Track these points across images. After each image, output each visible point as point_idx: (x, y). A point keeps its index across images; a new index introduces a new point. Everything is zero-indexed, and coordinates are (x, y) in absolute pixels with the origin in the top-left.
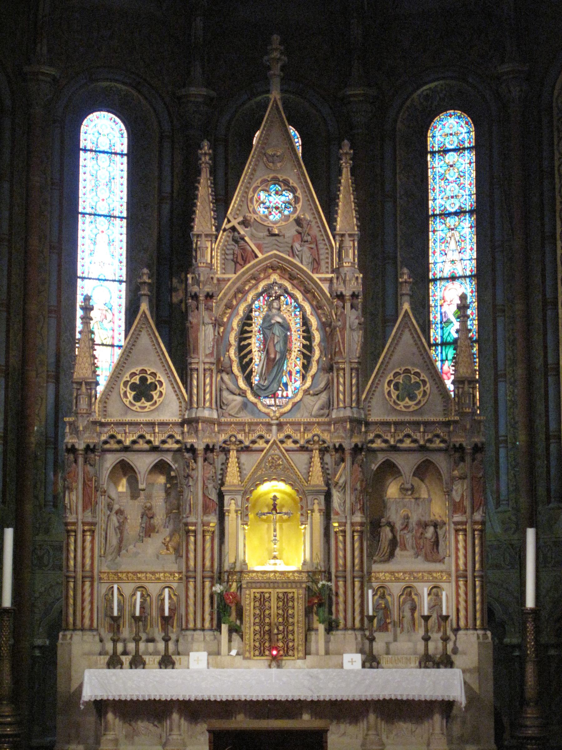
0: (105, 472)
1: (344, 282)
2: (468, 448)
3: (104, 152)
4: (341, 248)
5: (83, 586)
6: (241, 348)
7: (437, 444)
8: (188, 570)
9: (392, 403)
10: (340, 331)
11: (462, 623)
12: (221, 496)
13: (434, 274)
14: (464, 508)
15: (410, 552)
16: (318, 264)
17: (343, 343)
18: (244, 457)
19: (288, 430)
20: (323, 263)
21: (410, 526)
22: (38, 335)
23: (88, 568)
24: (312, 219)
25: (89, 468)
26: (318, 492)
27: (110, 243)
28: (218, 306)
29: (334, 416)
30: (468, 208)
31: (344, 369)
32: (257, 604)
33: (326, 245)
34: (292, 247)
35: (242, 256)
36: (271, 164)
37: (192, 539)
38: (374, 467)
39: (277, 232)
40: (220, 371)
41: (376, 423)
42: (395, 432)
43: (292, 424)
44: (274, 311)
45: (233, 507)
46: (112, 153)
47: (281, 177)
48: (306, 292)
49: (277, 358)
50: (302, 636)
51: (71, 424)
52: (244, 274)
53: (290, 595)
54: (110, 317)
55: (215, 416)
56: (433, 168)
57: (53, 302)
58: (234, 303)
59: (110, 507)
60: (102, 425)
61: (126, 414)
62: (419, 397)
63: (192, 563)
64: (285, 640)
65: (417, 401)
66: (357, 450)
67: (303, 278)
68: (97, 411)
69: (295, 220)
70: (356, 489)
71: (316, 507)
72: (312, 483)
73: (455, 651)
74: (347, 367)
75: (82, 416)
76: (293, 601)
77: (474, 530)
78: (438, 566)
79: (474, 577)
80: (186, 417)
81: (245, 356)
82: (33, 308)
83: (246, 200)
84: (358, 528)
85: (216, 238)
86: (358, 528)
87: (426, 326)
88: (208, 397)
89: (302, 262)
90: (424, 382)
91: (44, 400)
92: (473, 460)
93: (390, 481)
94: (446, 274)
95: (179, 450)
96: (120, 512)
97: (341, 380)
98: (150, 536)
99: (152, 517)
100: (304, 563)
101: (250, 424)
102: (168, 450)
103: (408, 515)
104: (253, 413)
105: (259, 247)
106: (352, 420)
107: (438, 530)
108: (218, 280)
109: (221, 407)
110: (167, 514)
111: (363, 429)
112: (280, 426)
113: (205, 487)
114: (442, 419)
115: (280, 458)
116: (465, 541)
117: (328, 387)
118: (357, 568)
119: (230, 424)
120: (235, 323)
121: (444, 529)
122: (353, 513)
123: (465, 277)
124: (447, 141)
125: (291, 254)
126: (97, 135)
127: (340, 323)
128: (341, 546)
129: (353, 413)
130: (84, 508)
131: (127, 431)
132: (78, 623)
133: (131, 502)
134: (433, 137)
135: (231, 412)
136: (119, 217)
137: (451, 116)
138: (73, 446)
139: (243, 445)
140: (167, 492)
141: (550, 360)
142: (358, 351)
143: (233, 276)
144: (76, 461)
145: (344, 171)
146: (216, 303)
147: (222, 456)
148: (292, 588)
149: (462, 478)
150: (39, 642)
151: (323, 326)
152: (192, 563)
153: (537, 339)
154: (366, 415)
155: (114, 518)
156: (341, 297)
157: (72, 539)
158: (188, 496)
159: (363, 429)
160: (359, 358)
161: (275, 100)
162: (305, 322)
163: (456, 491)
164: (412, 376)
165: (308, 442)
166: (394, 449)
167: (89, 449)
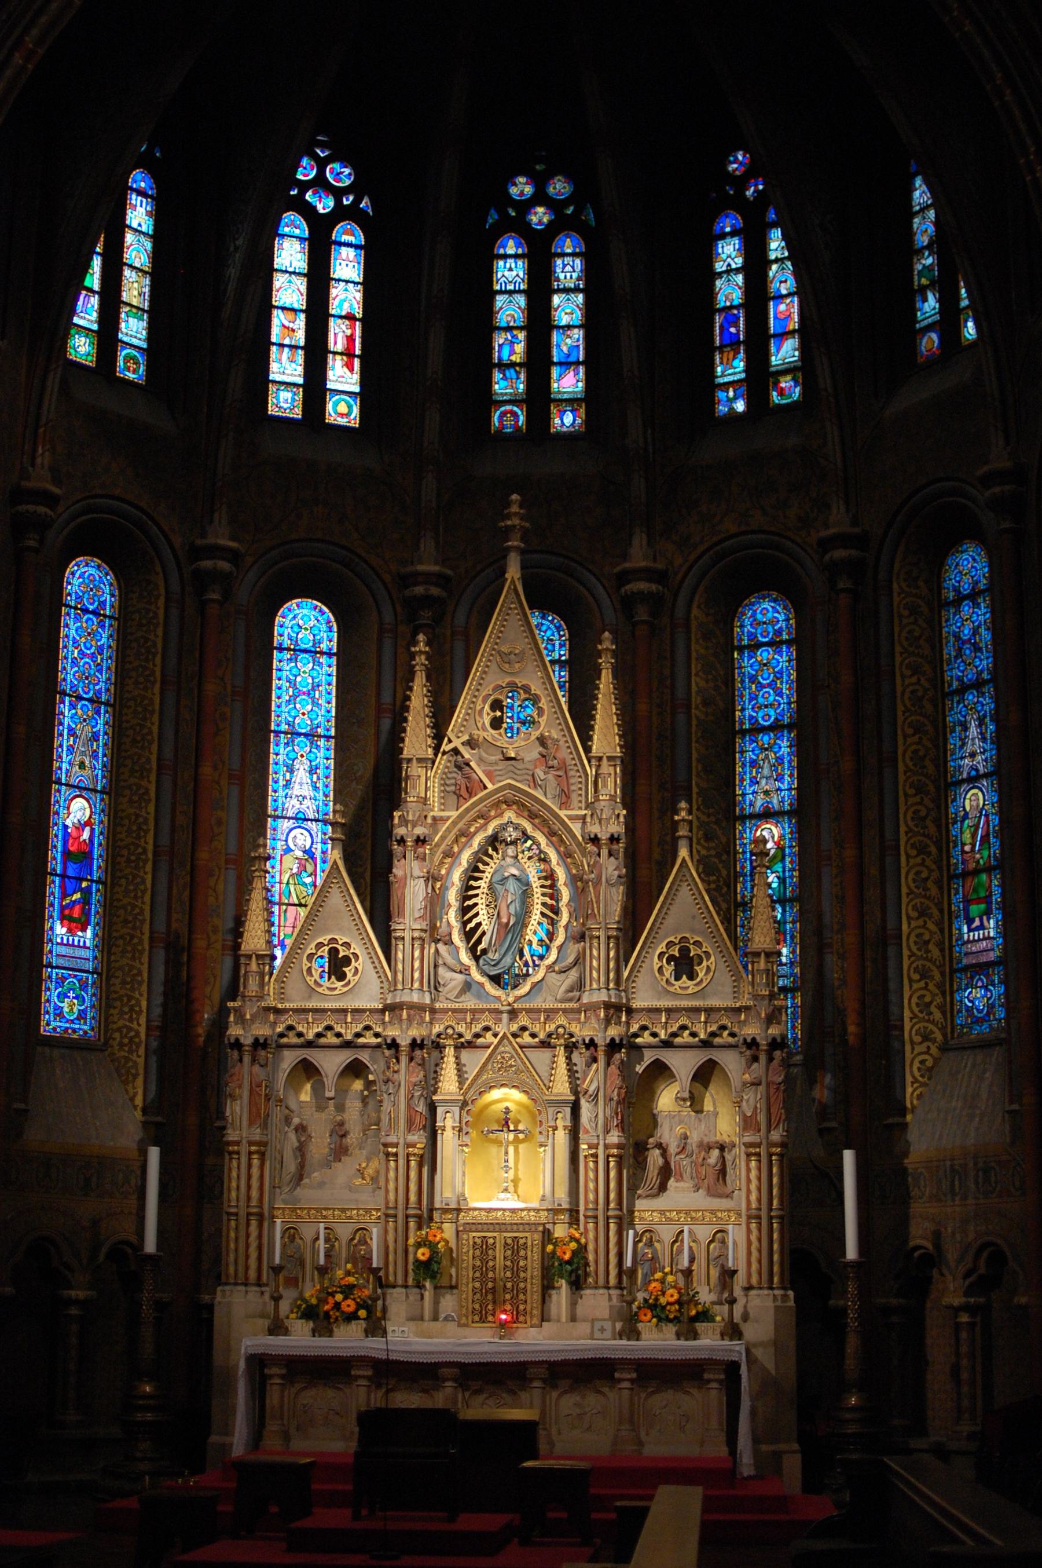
0: (281, 1074)
1: (600, 820)
2: (763, 1043)
3: (305, 651)
4: (597, 775)
5: (248, 1225)
6: (464, 910)
7: (725, 1038)
8: (387, 1208)
9: (664, 983)
10: (594, 888)
11: (754, 1281)
12: (432, 1108)
13: (742, 809)
14: (758, 1124)
15: (687, 1184)
16: (568, 797)
17: (598, 902)
18: (465, 1055)
19: (524, 1020)
20: (574, 797)
21: (688, 1148)
22: (211, 892)
23: (254, 1203)
24: (560, 738)
25: (256, 1068)
26: (564, 1103)
27: (312, 771)
28: (432, 854)
29: (585, 1001)
30: (786, 720)
31: (598, 937)
32: (478, 1252)
33: (578, 771)
34: (533, 775)
35: (467, 788)
36: (507, 666)
37: (392, 1164)
38: (639, 1069)
39: (513, 755)
40: (437, 941)
41: (643, 1010)
42: (666, 1023)
43: (529, 1011)
44: (509, 860)
45: (449, 1123)
46: (316, 652)
47: (520, 681)
48: (551, 834)
49: (511, 923)
50: (537, 1297)
51: (236, 1010)
52: (468, 810)
53: (522, 1241)
54: (310, 868)
55: (428, 1001)
56: (741, 668)
57: (232, 848)
58: (456, 849)
59: (288, 1120)
60: (277, 1011)
61: (310, 997)
62: (701, 975)
63: (392, 1196)
65: (698, 980)
66: (613, 1047)
67: (547, 815)
68: (272, 994)
69: (538, 738)
70: (611, 1099)
71: (560, 1123)
72: (555, 1091)
73: (745, 1317)
74: (602, 934)
75: (250, 1000)
76: (526, 1249)
77: (771, 1155)
78: (725, 1203)
79: (771, 1218)
80: (389, 1002)
81: (470, 920)
82: (203, 855)
84: (615, 1151)
85: (433, 763)
86: (615, 1151)
88: (417, 975)
89: (545, 794)
90: (708, 955)
91: (218, 978)
92: (770, 1059)
93: (662, 1087)
95: (378, 1046)
96: (301, 1129)
97: (595, 953)
98: (340, 1160)
99: (344, 1136)
100: (543, 1198)
101: (474, 1011)
102: (364, 1046)
103: (686, 1134)
104: (478, 996)
105: (489, 775)
106: (607, 1006)
107: (726, 1154)
108: (434, 818)
109: (436, 989)
110: (364, 1131)
111: (624, 1019)
112: (513, 1014)
113: (410, 1098)
114: (730, 1003)
115: (512, 1057)
116: (759, 1169)
118: (612, 1205)
119: (445, 1011)
120: (457, 876)
121: (733, 1152)
122: (607, 1131)
124: (759, 631)
125: (532, 784)
126: (296, 629)
127: (593, 876)
128: (591, 1175)
129: (610, 996)
130: (251, 1123)
131: (310, 1020)
132: (241, 1275)
133: (317, 1115)
134: (742, 626)
135: (448, 996)
136: (325, 736)
137: (764, 598)
138: (237, 1040)
139: (462, 1040)
140: (364, 1100)
142: (617, 913)
143: (454, 814)
144: (241, 1060)
145: (604, 672)
146: (430, 849)
147: (435, 1054)
148: (524, 1231)
149: (756, 1084)
151: (576, 880)
152: (392, 1196)
154: (628, 1000)
155: (292, 1136)
156: (595, 840)
157: (235, 1163)
159: (624, 1019)
160: (618, 922)
161: (513, 582)
163: (748, 1101)
164: (691, 947)
165: (550, 1035)
167: (259, 1044)
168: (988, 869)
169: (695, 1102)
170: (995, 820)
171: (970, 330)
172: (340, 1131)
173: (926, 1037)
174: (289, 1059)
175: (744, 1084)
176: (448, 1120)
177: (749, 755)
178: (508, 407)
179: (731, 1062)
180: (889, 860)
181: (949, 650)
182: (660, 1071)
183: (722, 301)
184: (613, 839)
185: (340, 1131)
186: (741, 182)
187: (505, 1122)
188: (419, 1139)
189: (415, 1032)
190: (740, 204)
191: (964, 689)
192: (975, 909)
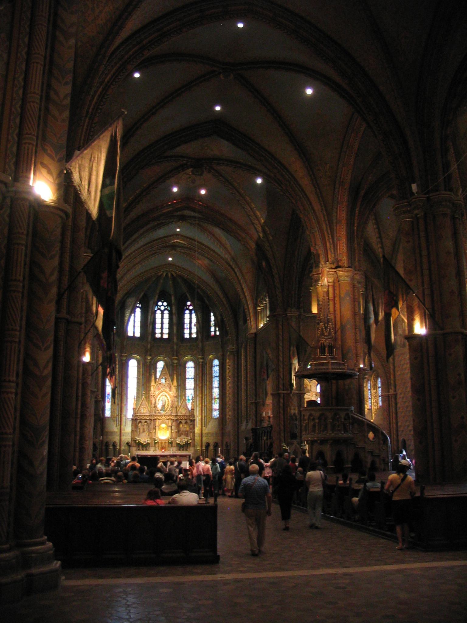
7: (188, 419)
12: (155, 426)
18: (159, 420)
60: (137, 415)
64: (165, 449)
66: (176, 420)
87: (185, 397)
117: (172, 410)
123: (191, 389)
149: (191, 424)
150: (123, 448)
153: (203, 401)
158: (150, 426)
166: (182, 420)
168: (217, 399)
170: (218, 393)
171: (218, 333)
172: (144, 429)
173: (209, 418)
174: (138, 421)
176: (157, 428)
179: (189, 422)
181: (213, 372)
182: (181, 423)
185: (144, 429)
186: (189, 306)
189: (154, 418)
190: (188, 309)
191: (215, 377)
192: (215, 403)
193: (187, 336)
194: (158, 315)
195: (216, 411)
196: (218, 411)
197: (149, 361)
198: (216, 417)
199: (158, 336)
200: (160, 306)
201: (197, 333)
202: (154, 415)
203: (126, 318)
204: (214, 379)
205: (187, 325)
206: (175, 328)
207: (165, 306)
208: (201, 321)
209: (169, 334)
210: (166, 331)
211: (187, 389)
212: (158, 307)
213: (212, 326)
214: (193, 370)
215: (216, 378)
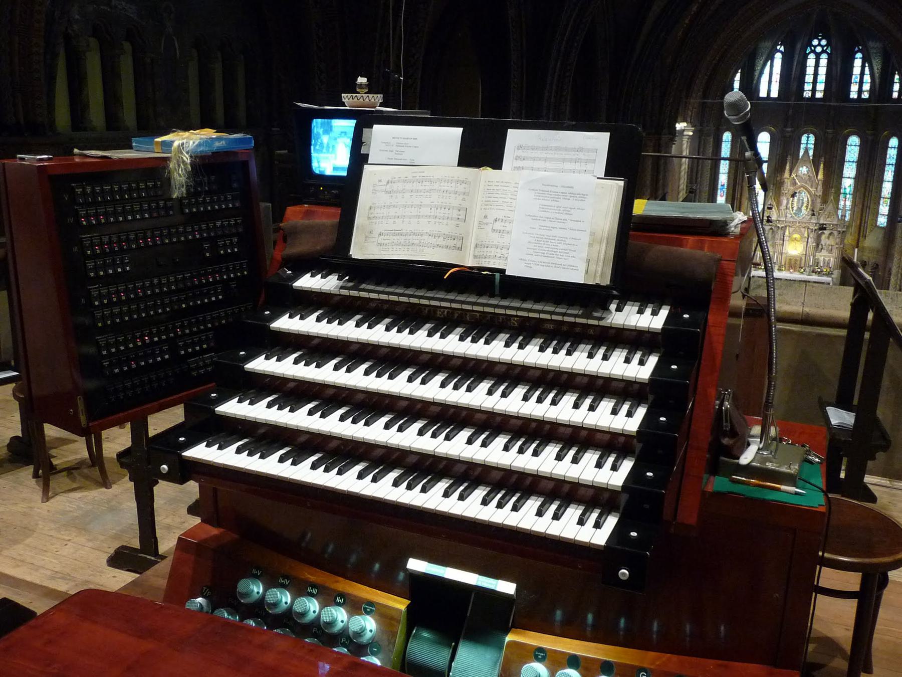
2: (841, 232)
18: (790, 228)
19: (801, 224)
26: (805, 238)
30: (855, 161)
83: (797, 170)
94: (848, 177)
112: (799, 223)
123: (852, 178)
141: (869, 204)
149: (839, 238)
153: (866, 199)
156: (817, 195)
158: (776, 236)
162: (808, 200)
168: (888, 198)
169: (828, 238)
170: (891, 191)
175: (837, 238)
177: (847, 166)
178: (808, 92)
179: (835, 233)
180: (870, 193)
181: (888, 156)
183: (854, 73)
184: (820, 195)
187: (796, 239)
188: (782, 242)
191: (889, 164)
192: (884, 205)
193: (854, 95)
194: (811, 61)
195: (883, 217)
196: (886, 217)
197: (788, 135)
198: (882, 226)
199: (807, 94)
200: (815, 47)
201: (871, 91)
202: (783, 221)
203: (757, 74)
204: (887, 168)
205: (855, 78)
206: (834, 85)
207: (823, 47)
208: (877, 75)
209: (825, 91)
210: (821, 87)
211: (844, 177)
212: (811, 49)
213: (896, 82)
214: (857, 149)
215: (891, 166)
